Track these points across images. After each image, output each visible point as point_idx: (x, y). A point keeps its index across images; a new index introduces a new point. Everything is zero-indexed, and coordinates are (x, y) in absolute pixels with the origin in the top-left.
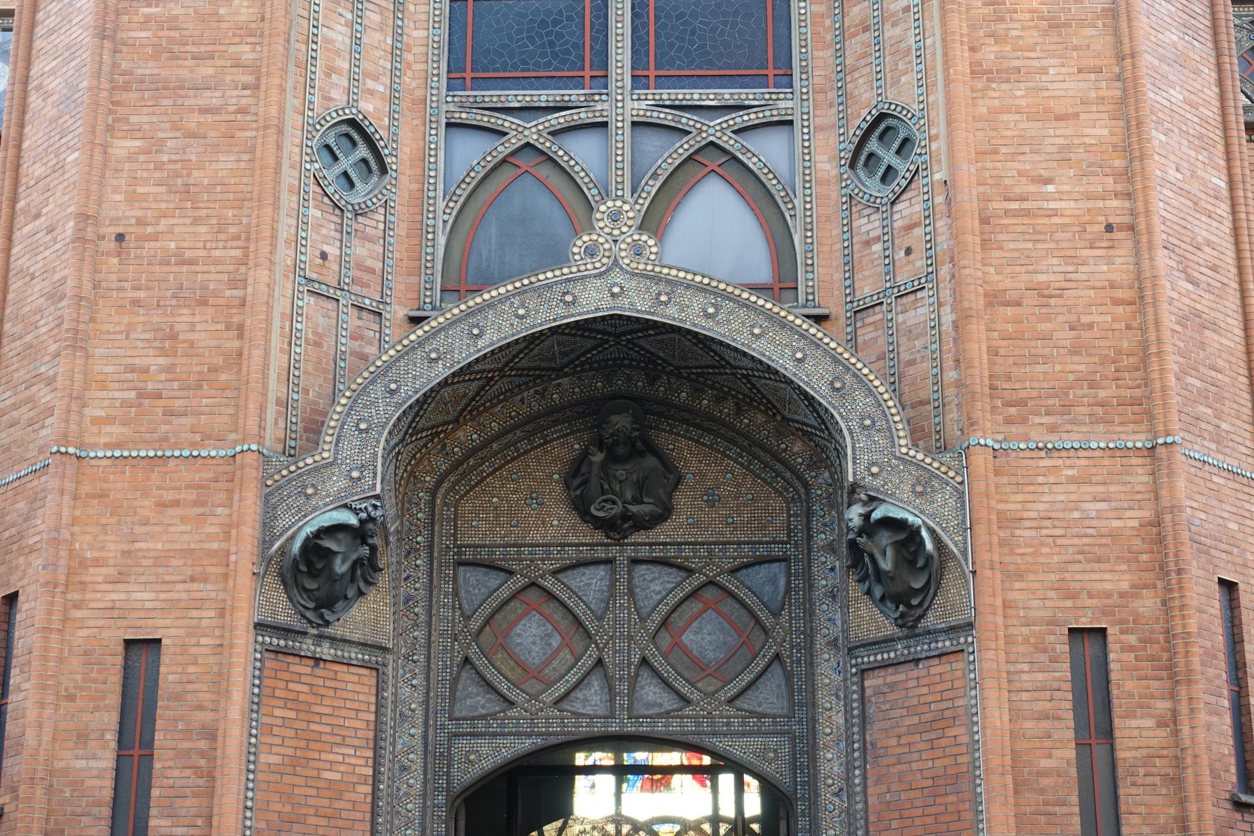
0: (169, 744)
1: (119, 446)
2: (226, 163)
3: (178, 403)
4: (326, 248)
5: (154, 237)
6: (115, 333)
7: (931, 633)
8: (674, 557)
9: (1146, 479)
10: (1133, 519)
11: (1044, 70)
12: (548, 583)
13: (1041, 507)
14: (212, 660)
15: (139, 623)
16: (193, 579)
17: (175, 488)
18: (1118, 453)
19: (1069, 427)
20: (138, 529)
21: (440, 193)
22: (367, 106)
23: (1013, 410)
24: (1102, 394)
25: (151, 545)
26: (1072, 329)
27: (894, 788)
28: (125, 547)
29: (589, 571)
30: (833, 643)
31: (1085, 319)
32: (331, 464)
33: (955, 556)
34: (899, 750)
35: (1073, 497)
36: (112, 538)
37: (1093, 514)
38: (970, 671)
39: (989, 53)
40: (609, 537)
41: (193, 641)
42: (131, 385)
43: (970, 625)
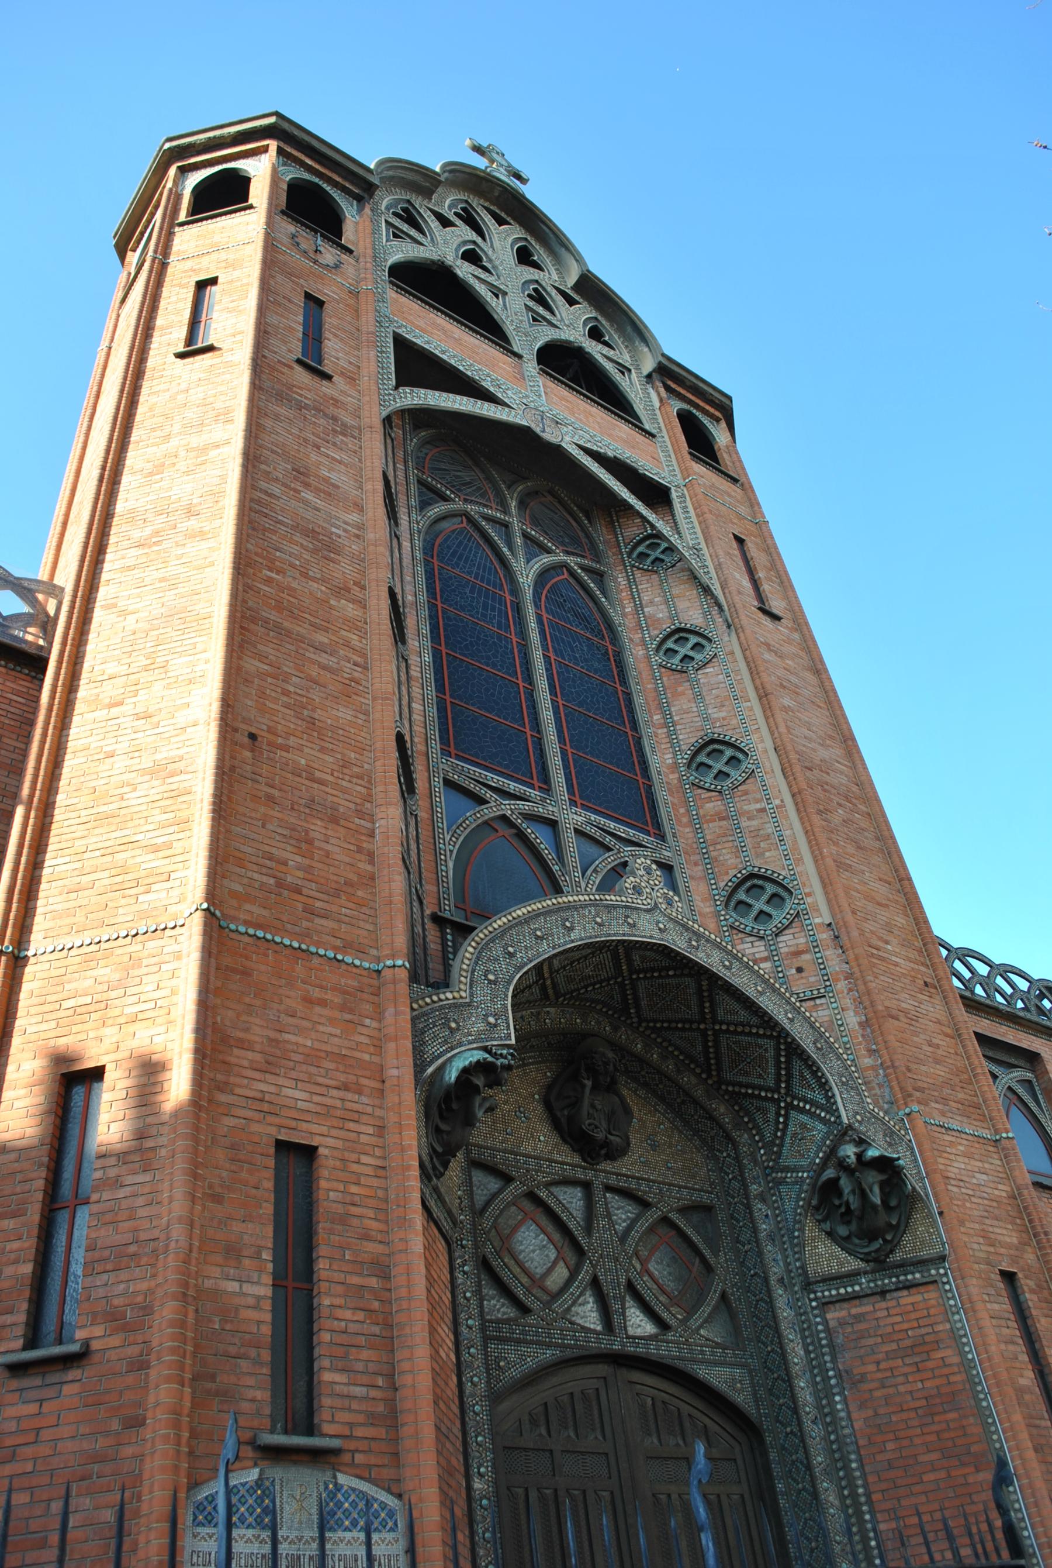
0: (338, 1277)
1: (258, 926)
3: (318, 904)
6: (250, 817)
7: (904, 1266)
8: (635, 1189)
12: (543, 1194)
14: (375, 1182)
15: (293, 1124)
16: (345, 1087)
17: (321, 987)
18: (981, 1141)
19: (950, 1115)
20: (285, 1019)
25: (300, 1040)
27: (881, 1411)
28: (272, 1034)
29: (570, 1190)
30: (781, 1280)
32: (469, 1005)
33: (922, 1199)
34: (880, 1375)
36: (258, 1021)
38: (949, 1299)
40: (585, 1161)
41: (353, 1157)
42: (270, 872)
43: (943, 1258)
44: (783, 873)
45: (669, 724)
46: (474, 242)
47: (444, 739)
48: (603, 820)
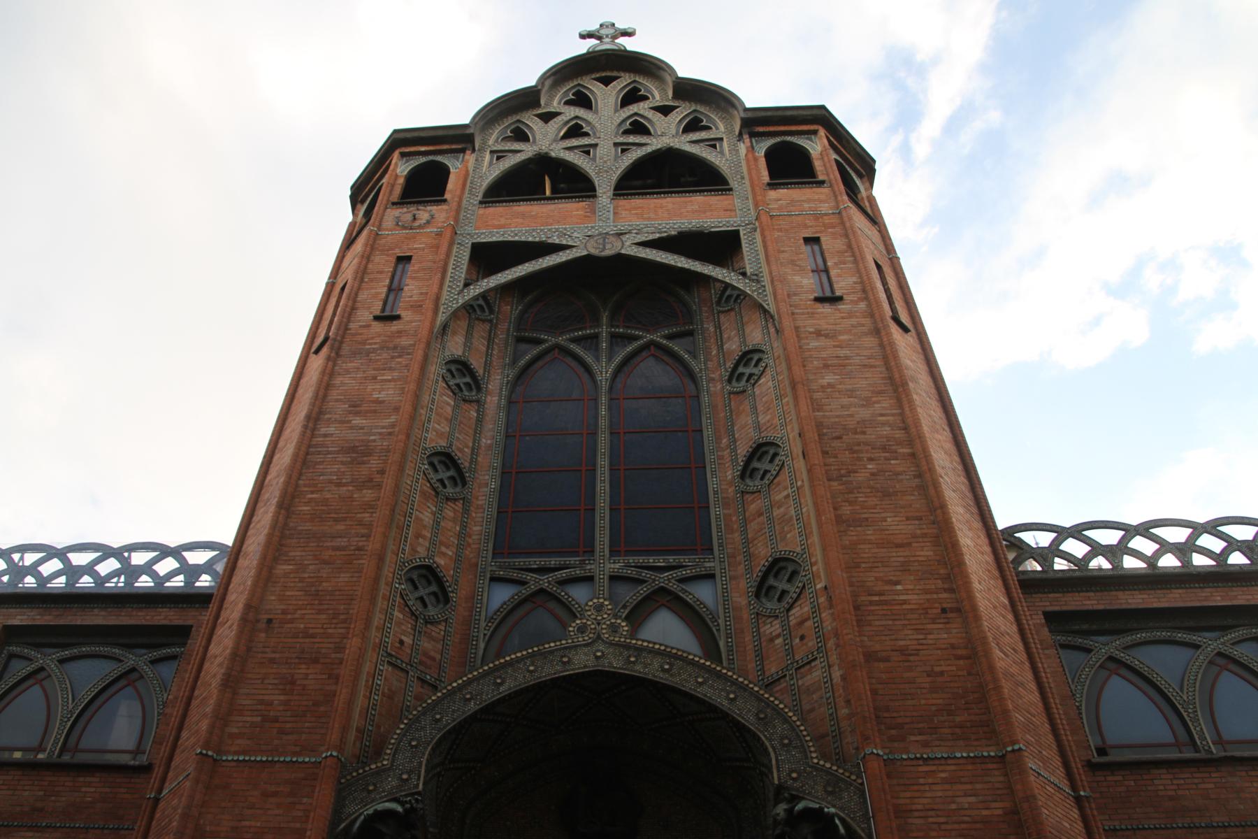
4: (403, 638)
9: (1001, 779)
10: (997, 809)
13: (925, 801)
19: (937, 743)
21: (483, 618)
22: (441, 561)
23: (893, 732)
24: (958, 719)
26: (929, 676)
31: (937, 669)
35: (950, 793)
37: (966, 806)
39: (846, 510)
44: (798, 549)
46: (577, 117)
48: (641, 560)
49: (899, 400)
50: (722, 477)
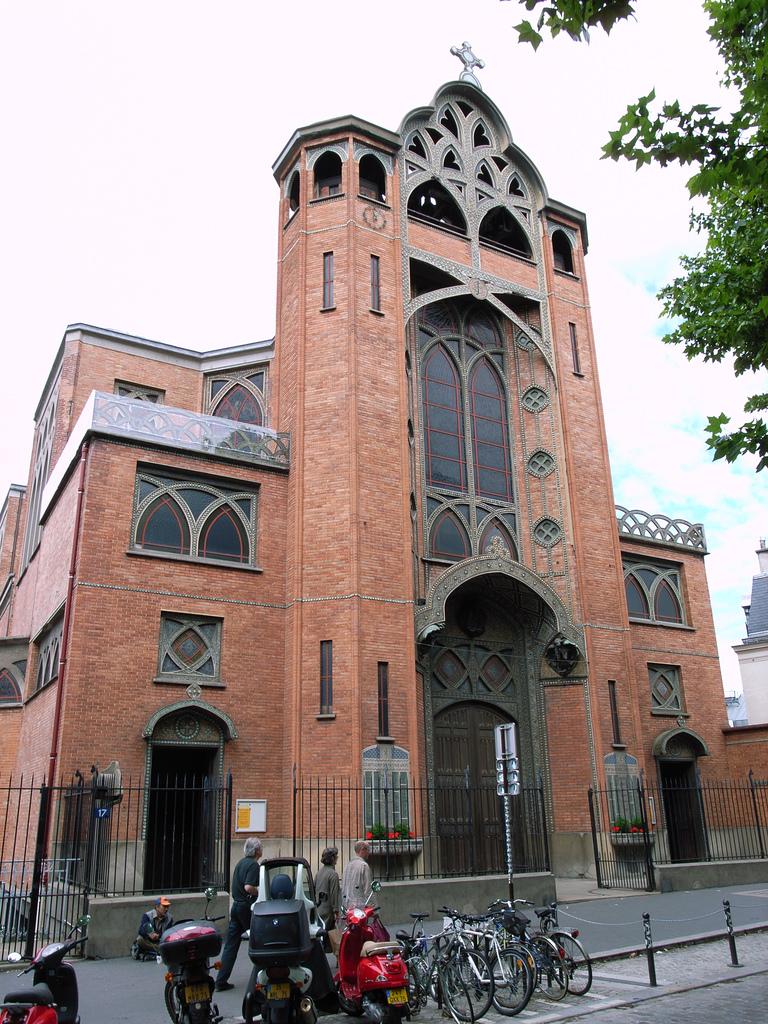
2: (394, 503)
5: (375, 525)
7: (570, 678)
11: (593, 517)
12: (453, 649)
45: (523, 440)
47: (428, 478)
49: (603, 451)
50: (518, 460)
